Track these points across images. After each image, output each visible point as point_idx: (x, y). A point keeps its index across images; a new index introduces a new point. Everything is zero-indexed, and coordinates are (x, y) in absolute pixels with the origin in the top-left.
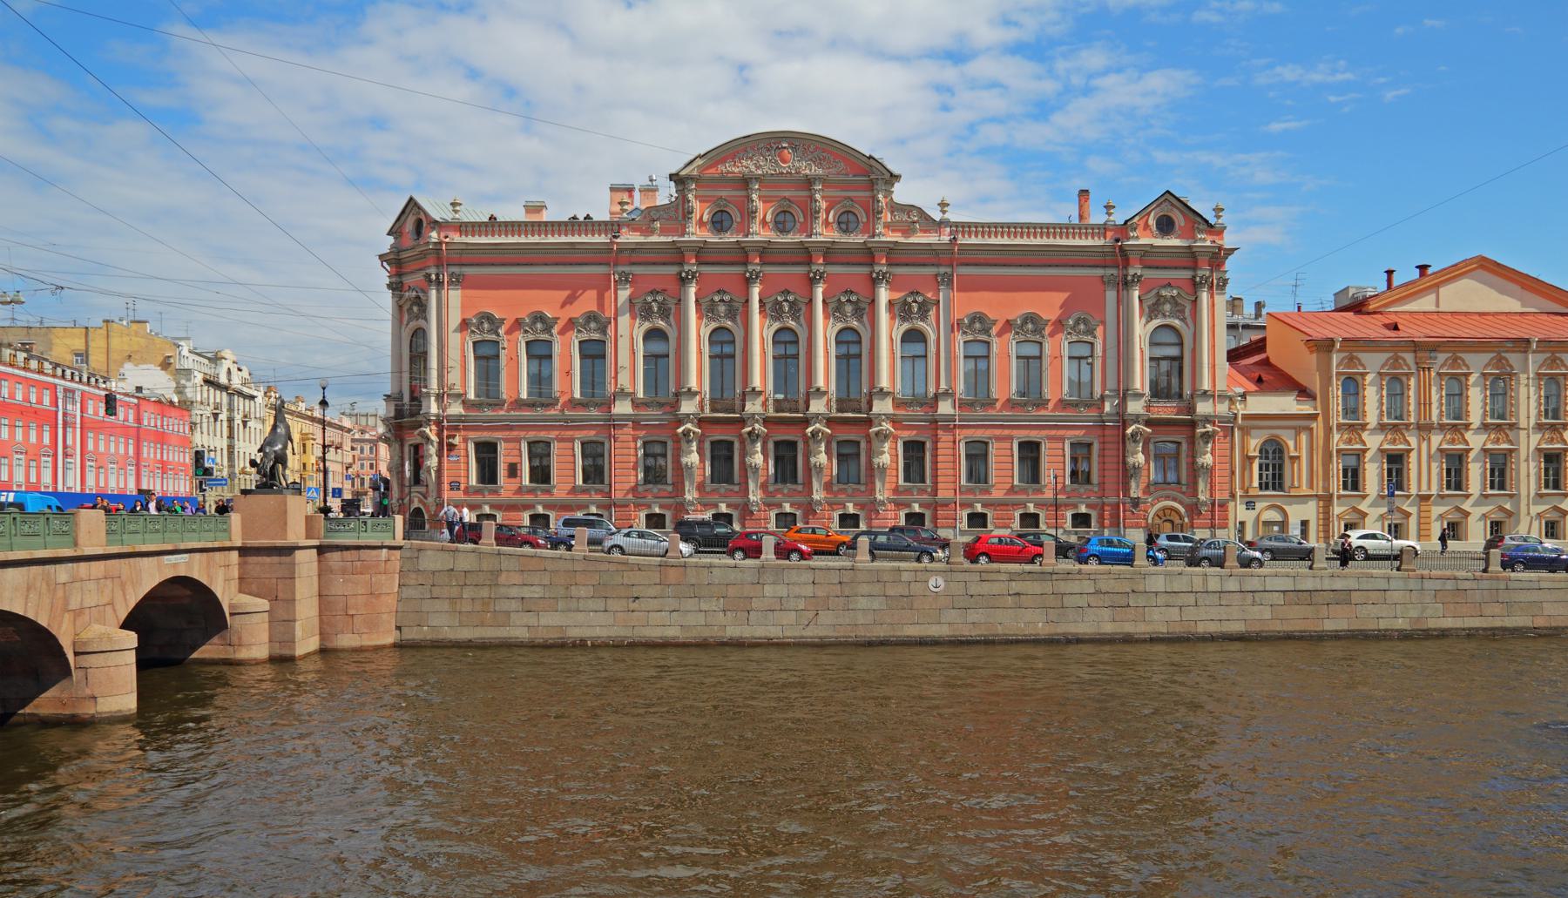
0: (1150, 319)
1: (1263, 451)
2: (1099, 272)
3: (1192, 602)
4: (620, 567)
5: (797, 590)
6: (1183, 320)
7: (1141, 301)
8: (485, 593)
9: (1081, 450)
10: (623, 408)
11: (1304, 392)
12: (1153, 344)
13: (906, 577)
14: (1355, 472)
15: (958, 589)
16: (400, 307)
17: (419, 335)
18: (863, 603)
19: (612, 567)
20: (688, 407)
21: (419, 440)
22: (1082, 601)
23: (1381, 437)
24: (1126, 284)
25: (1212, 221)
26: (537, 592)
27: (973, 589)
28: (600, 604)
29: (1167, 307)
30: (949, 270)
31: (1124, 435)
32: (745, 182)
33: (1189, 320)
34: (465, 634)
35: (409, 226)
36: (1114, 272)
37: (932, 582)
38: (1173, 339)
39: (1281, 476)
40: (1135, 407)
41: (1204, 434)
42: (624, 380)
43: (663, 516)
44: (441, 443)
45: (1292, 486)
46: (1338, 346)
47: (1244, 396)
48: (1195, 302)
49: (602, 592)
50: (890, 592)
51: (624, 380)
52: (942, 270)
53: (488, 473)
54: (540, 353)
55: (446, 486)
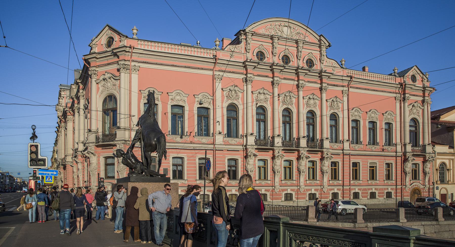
2: (395, 95)
6: (419, 116)
29: (415, 111)
36: (399, 95)
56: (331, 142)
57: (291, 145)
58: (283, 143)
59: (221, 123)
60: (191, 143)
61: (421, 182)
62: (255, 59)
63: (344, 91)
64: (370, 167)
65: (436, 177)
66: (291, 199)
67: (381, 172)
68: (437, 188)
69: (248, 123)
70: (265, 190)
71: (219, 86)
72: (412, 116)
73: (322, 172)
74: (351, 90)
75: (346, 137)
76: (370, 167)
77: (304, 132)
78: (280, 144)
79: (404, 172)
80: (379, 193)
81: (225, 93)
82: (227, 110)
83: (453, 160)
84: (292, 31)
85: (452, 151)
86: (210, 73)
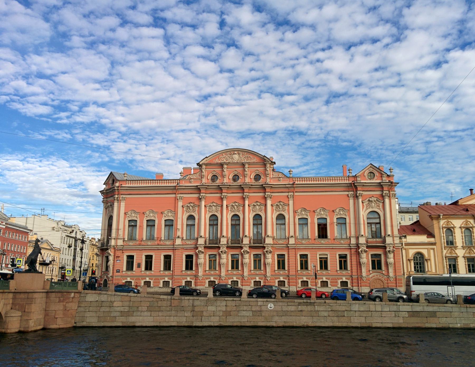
0: (367, 209)
1: (415, 258)
2: (347, 193)
3: (370, 315)
4: (157, 300)
5: (219, 308)
6: (379, 209)
7: (362, 203)
8: (108, 309)
9: (343, 258)
10: (178, 242)
11: (431, 235)
12: (367, 218)
13: (259, 304)
14: (455, 266)
15: (279, 308)
16: (106, 209)
17: (111, 218)
18: (244, 313)
19: (155, 300)
20: (201, 241)
21: (107, 255)
22: (326, 314)
23: (464, 251)
24: (356, 197)
25: (389, 174)
26: (127, 309)
27: (285, 309)
28: (149, 314)
30: (292, 194)
31: (359, 252)
32: (221, 165)
33: (382, 210)
34: (102, 324)
35: (111, 182)
36: (352, 193)
37: (269, 306)
38: (377, 216)
39: (424, 267)
40: (362, 241)
41: (389, 251)
42: (179, 233)
44: (114, 256)
45: (428, 271)
46: (441, 217)
47: (405, 237)
48: (384, 203)
49: (150, 309)
50: (254, 309)
51: (179, 233)
52: (290, 194)
53: (130, 266)
54: (151, 224)
55: (115, 271)
57: (235, 243)
59: (180, 230)
60: (158, 245)
61: (384, 272)
63: (289, 196)
64: (320, 258)
67: (333, 263)
70: (214, 278)
74: (296, 194)
75: (292, 233)
76: (320, 258)
80: (331, 282)
81: (185, 208)
82: (210, 220)
83: (433, 249)
84: (241, 156)
85: (432, 240)
86: (174, 196)
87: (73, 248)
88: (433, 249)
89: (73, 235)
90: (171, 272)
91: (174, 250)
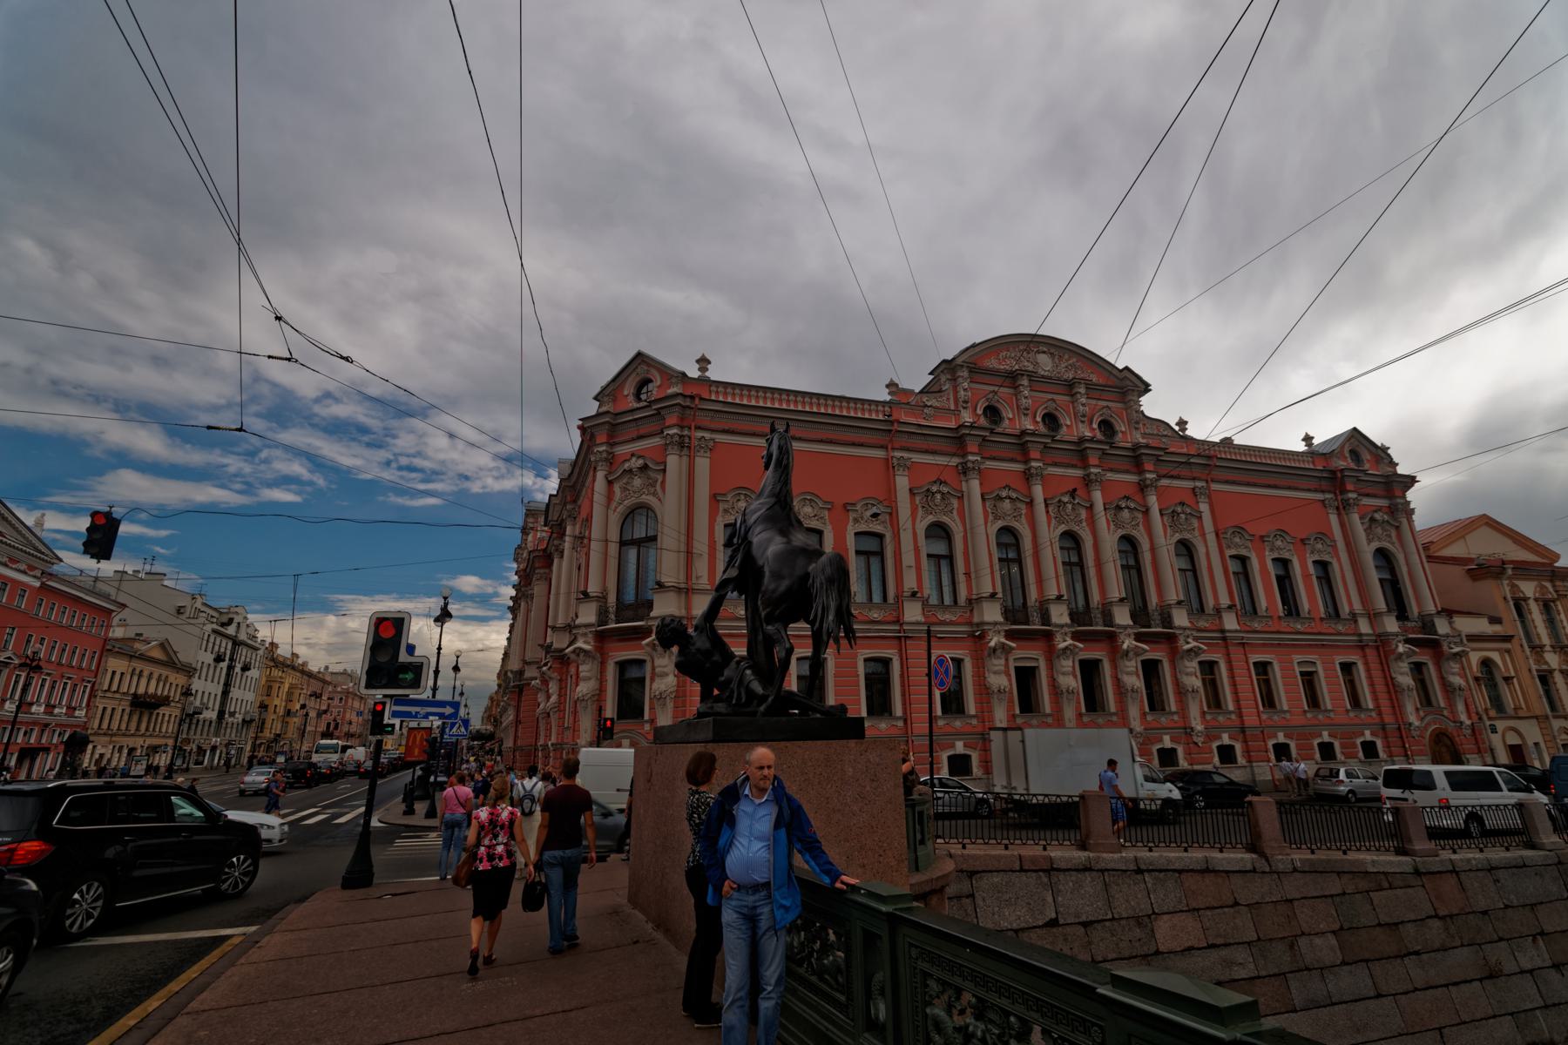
2: (1320, 496)
24: (1343, 508)
35: (629, 389)
43: (968, 757)
46: (1510, 572)
51: (910, 583)
56: (1190, 613)
57: (1089, 622)
58: (1071, 615)
62: (983, 421)
65: (1481, 699)
66: (1174, 762)
68: (1494, 731)
69: (984, 572)
71: (902, 482)
72: (1376, 545)
73: (1181, 692)
75: (1225, 601)
77: (1116, 590)
78: (1066, 619)
79: (1393, 689)
81: (918, 499)
83: (1508, 651)
86: (880, 453)
87: (224, 665)
88: (1508, 651)
89: (231, 630)
90: (900, 724)
91: (901, 640)
